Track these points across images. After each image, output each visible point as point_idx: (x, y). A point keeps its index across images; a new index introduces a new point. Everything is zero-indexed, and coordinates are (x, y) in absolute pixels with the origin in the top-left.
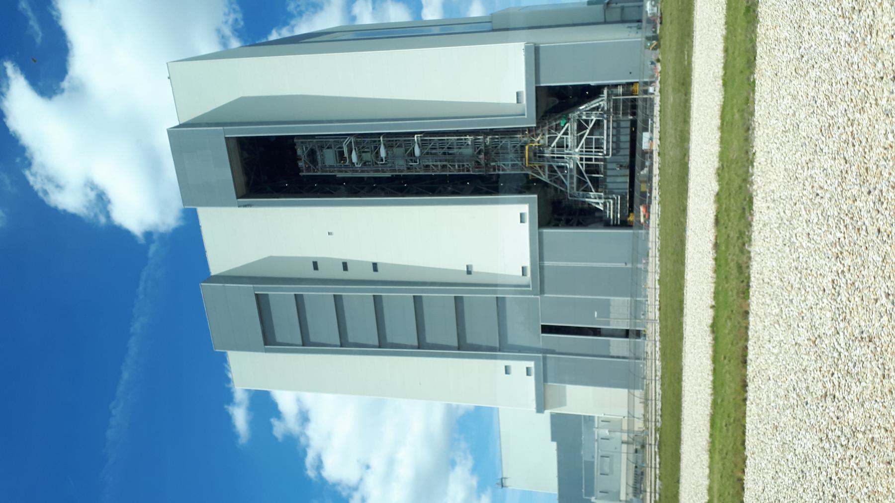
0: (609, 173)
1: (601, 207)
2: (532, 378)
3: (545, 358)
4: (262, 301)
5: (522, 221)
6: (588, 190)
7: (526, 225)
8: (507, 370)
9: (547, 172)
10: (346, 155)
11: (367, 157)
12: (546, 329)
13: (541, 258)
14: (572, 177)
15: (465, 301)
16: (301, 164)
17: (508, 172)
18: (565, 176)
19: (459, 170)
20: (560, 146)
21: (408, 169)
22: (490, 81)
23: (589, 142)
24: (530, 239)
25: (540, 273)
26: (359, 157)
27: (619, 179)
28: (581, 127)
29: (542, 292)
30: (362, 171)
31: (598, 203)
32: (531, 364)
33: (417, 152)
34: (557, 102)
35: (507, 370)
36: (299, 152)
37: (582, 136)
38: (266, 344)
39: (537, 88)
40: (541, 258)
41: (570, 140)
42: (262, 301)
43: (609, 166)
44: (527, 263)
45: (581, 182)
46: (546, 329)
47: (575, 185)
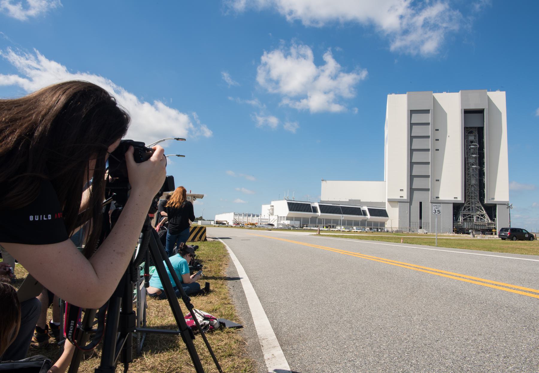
4: (427, 111)
7: (454, 199)
11: (472, 150)
12: (421, 203)
13: (443, 203)
22: (500, 190)
23: (478, 218)
25: (436, 202)
28: (482, 215)
32: (405, 197)
34: (491, 210)
38: (411, 111)
40: (443, 203)
42: (427, 111)
44: (440, 199)
46: (421, 203)
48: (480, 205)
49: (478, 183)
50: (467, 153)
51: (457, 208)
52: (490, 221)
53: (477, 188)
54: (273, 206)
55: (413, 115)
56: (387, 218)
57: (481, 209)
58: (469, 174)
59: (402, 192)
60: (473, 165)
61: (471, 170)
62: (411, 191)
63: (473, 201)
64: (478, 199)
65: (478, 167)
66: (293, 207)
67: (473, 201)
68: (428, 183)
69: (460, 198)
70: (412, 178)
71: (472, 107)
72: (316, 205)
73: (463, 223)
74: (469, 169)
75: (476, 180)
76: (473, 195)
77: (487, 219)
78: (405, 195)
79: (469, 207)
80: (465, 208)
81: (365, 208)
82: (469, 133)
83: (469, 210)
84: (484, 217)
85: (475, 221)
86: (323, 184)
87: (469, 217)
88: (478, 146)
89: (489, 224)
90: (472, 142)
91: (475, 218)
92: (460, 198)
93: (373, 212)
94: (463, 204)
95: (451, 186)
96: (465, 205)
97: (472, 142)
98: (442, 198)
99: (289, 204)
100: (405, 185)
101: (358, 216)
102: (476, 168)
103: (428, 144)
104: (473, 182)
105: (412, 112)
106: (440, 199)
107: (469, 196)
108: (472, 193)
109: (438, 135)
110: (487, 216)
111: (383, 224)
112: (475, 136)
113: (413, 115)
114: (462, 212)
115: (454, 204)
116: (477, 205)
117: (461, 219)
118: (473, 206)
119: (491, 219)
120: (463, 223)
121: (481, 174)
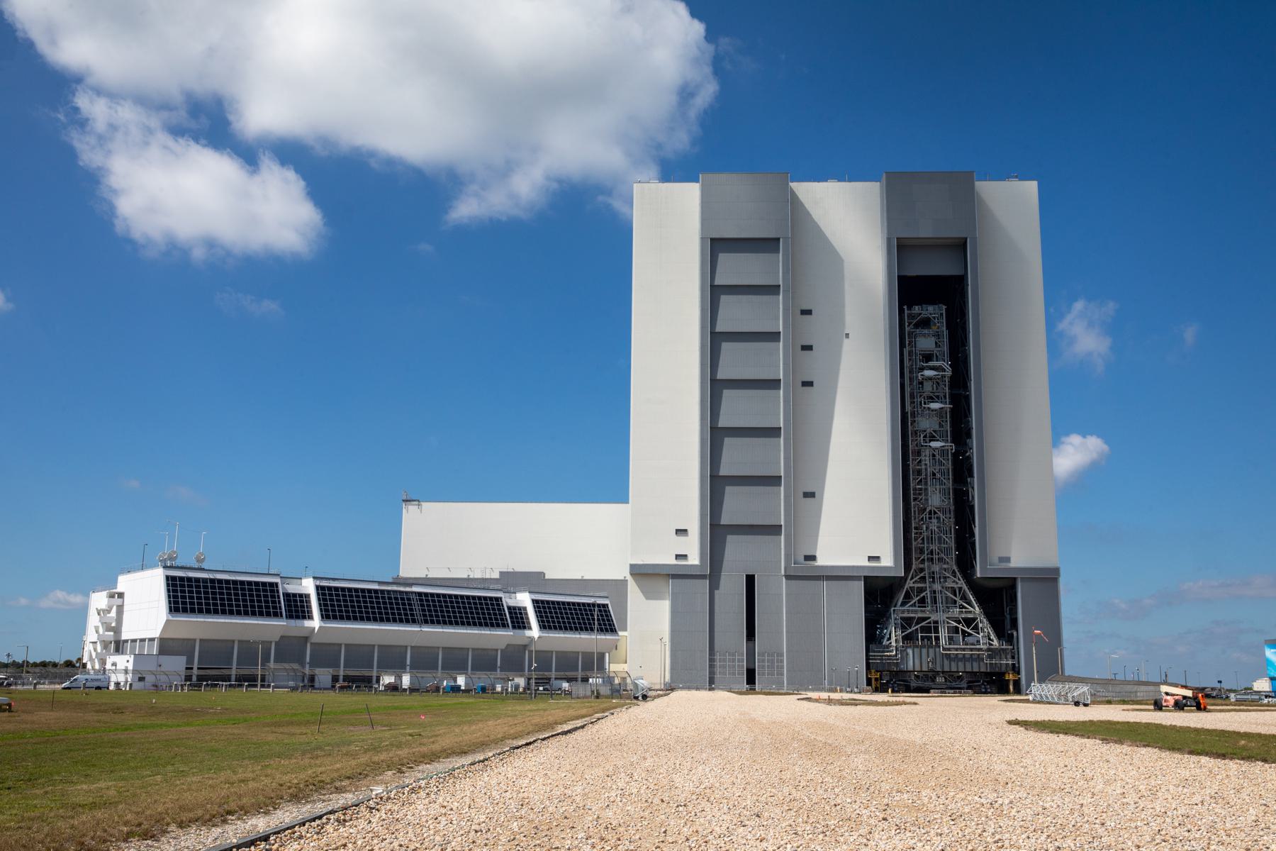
0: (924, 651)
1: (885, 642)
2: (672, 561)
3: (702, 577)
5: (871, 558)
6: (903, 628)
8: (681, 532)
10: (931, 364)
11: (928, 387)
12: (750, 580)
13: (830, 578)
14: (913, 612)
15: (775, 488)
16: (916, 309)
17: (914, 543)
18: (914, 605)
19: (915, 489)
21: (916, 432)
23: (956, 630)
24: (853, 567)
25: (807, 574)
26: (930, 379)
27: (917, 662)
28: (969, 622)
29: (788, 577)
30: (911, 379)
31: (889, 639)
32: (694, 559)
33: (934, 444)
34: (998, 599)
35: (681, 532)
36: (931, 308)
37: (959, 622)
39: (1015, 579)
40: (830, 578)
41: (956, 612)
43: (931, 651)
44: (821, 562)
45: (907, 622)
46: (750, 580)
47: (906, 615)
48: (962, 583)
49: (950, 504)
50: (912, 396)
51: (880, 594)
52: (995, 643)
53: (950, 521)
54: (121, 595)
55: (722, 257)
56: (609, 637)
57: (964, 598)
58: (919, 472)
59: (682, 538)
60: (933, 438)
61: (926, 458)
62: (717, 533)
63: (936, 568)
65: (951, 447)
66: (186, 594)
67: (936, 568)
68: (776, 506)
69: (888, 560)
70: (716, 485)
71: (925, 230)
72: (308, 586)
73: (903, 651)
74: (919, 453)
75: (944, 492)
76: (934, 547)
77: (985, 637)
78: (693, 551)
79: (921, 590)
80: (908, 596)
81: (524, 600)
82: (917, 326)
83: (922, 601)
84: (976, 628)
85: (943, 642)
86: (410, 514)
87: (924, 629)
88: (949, 373)
89: (993, 653)
90: (928, 357)
91: (943, 634)
92: (888, 560)
93: (553, 615)
94: (902, 581)
95: (856, 521)
96: (909, 584)
97: (928, 357)
98: (826, 558)
99: (172, 583)
100: (691, 513)
101: (486, 632)
102: (943, 451)
103: (776, 362)
104: (936, 499)
105: (716, 247)
106: (821, 562)
107: (922, 551)
108: (930, 540)
109: (813, 330)
110: (984, 623)
111: (594, 663)
112: (938, 335)
113: (722, 257)
114: (899, 611)
115: (866, 578)
116: (949, 584)
117: (893, 636)
118: (937, 587)
119: (1000, 635)
120: (903, 651)
121: (962, 469)
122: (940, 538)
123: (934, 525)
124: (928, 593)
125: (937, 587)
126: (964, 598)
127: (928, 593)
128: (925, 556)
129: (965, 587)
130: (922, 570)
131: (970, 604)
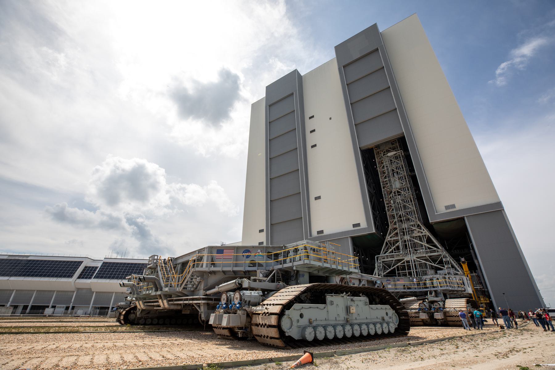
8: (261, 231)
9: (392, 239)
20: (415, 246)
63: (405, 226)
64: (415, 220)
67: (405, 226)
96: (388, 238)
115: (354, 239)
116: (416, 234)
122: (405, 207)
123: (399, 199)
124: (400, 244)
125: (407, 237)
126: (429, 241)
127: (400, 244)
128: (396, 220)
129: (428, 234)
130: (396, 229)
131: (435, 246)
